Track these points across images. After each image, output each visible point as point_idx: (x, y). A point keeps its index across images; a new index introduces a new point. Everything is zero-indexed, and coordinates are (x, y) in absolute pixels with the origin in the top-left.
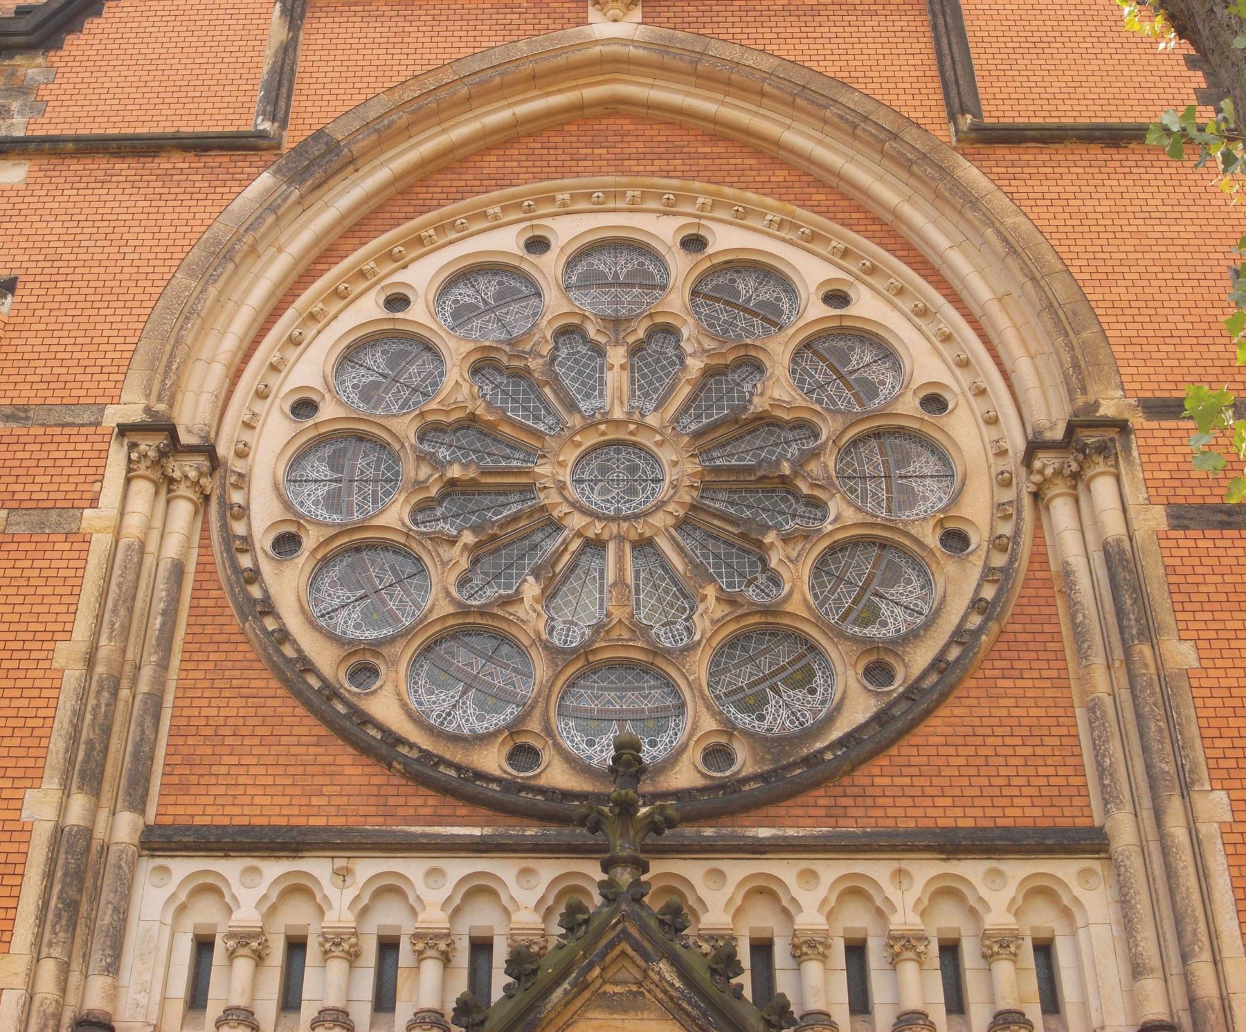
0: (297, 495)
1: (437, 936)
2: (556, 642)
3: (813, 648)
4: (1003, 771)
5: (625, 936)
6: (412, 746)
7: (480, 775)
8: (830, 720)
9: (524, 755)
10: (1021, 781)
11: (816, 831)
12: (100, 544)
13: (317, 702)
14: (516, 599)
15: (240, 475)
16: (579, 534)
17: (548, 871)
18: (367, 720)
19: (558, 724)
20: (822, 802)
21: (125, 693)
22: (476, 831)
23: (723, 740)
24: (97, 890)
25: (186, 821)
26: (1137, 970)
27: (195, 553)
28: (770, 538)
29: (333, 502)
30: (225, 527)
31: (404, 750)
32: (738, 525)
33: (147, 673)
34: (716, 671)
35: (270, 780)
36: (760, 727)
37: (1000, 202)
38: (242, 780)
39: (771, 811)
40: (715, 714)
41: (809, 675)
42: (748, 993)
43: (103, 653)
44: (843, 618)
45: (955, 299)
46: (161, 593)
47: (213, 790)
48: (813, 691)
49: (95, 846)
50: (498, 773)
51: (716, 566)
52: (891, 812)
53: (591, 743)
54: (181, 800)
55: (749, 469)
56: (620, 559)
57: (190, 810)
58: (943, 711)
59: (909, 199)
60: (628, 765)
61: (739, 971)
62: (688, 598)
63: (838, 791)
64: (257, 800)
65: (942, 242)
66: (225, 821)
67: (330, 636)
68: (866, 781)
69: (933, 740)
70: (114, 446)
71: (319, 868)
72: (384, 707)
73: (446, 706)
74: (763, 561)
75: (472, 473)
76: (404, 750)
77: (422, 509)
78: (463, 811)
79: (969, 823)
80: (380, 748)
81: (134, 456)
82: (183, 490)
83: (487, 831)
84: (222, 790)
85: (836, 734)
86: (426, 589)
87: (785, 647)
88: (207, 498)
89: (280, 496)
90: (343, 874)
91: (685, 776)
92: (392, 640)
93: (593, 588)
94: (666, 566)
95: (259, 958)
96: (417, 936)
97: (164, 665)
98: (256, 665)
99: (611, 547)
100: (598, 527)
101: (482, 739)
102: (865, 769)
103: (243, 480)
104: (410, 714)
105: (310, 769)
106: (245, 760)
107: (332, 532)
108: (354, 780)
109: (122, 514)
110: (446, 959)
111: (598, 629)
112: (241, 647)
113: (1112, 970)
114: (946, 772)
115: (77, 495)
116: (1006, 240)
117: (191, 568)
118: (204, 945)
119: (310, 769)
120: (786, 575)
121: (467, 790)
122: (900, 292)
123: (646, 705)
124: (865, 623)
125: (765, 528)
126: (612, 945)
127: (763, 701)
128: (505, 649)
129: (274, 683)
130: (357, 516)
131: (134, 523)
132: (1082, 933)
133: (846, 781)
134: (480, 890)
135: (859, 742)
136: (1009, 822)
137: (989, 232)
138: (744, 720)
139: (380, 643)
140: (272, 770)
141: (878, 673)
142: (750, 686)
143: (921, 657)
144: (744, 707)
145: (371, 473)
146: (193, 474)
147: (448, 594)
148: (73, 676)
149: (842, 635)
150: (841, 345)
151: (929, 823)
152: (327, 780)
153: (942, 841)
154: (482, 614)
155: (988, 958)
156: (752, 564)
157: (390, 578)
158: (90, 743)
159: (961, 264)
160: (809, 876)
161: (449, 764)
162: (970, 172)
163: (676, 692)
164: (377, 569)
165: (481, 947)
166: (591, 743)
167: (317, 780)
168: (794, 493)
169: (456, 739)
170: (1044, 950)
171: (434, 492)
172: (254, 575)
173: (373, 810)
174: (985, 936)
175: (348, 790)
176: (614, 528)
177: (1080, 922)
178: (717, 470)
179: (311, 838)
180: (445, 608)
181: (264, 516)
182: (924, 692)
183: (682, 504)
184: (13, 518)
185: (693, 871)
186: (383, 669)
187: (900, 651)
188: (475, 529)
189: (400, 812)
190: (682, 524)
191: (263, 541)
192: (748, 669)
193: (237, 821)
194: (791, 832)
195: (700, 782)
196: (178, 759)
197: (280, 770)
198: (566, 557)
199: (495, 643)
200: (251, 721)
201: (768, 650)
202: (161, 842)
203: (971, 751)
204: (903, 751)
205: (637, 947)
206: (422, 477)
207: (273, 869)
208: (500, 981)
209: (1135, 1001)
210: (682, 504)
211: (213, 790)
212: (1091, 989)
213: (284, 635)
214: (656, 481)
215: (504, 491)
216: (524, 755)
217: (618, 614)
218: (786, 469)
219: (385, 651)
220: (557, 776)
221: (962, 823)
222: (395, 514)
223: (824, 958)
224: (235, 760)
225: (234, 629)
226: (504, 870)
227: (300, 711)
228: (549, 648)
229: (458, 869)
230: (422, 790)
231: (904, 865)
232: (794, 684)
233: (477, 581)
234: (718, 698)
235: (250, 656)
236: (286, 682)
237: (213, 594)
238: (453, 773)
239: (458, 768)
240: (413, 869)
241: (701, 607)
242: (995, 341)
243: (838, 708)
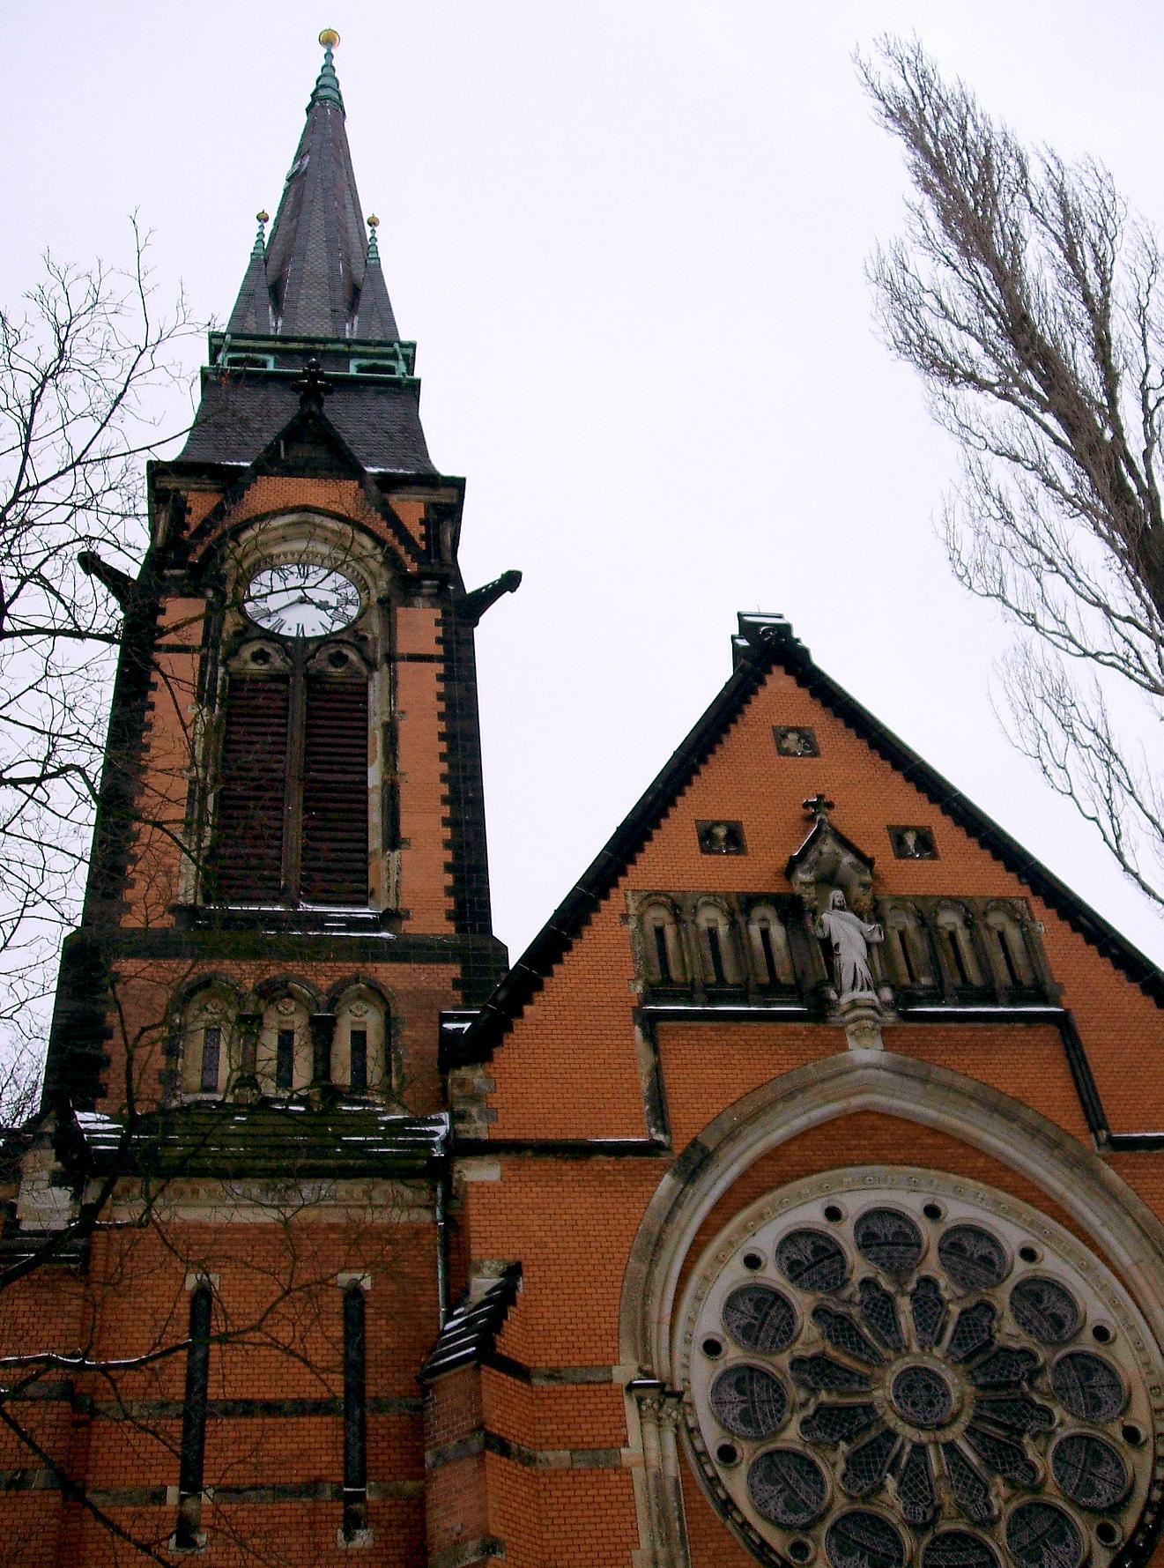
37: (1131, 1196)
45: (1104, 1258)
59: (1069, 1188)
65: (1097, 1223)
70: (626, 1400)
103: (694, 1413)
116: (1139, 1226)
122: (1069, 1253)
131: (653, 1455)
137: (1129, 1221)
150: (1043, 1299)
159: (1108, 1237)
162: (1109, 1173)
181: (712, 1437)
242: (1134, 1290)
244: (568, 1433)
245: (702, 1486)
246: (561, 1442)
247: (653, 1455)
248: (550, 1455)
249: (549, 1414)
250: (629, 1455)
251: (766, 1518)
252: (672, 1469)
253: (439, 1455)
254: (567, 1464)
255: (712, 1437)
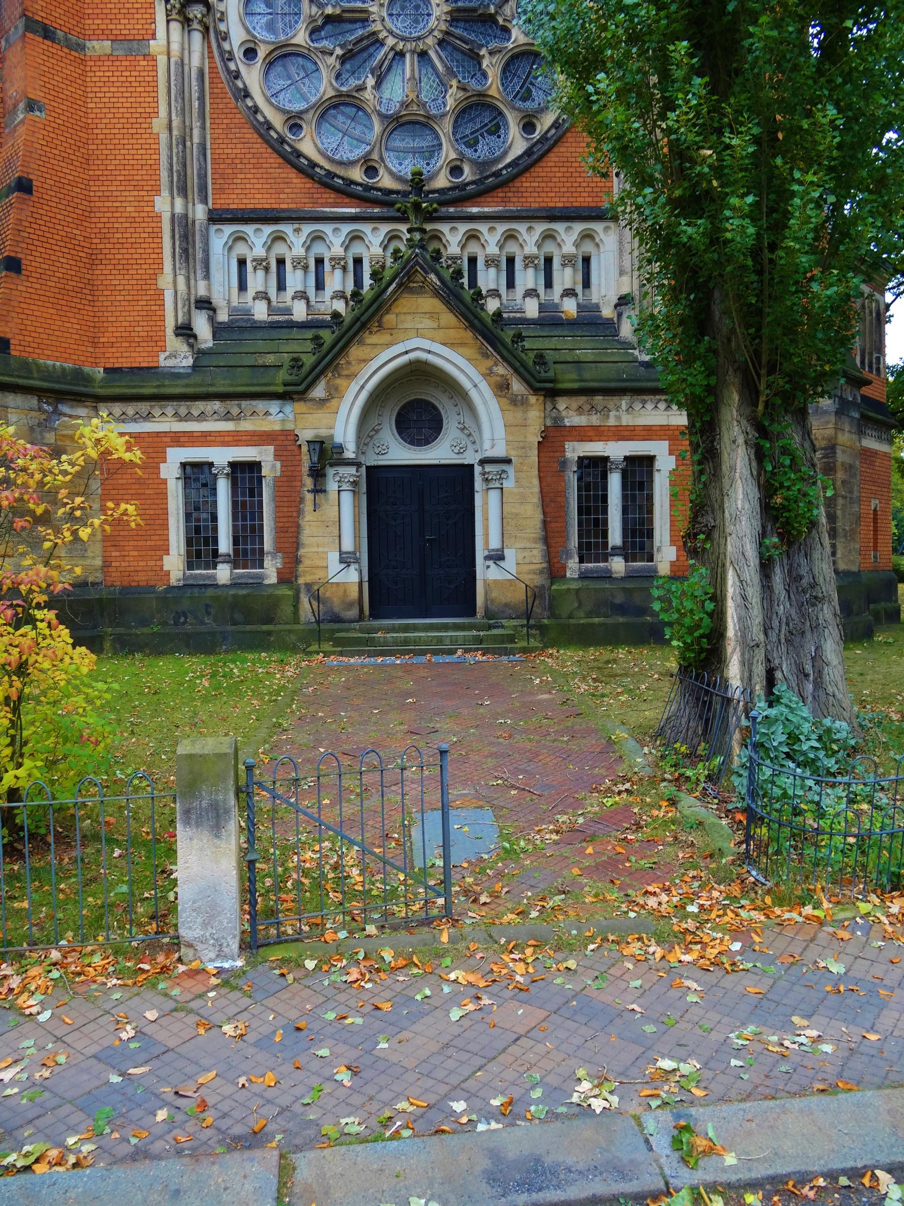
0: (251, 22)
1: (340, 259)
2: (383, 111)
3: (501, 113)
4: (578, 180)
5: (417, 263)
6: (322, 168)
7: (353, 182)
8: (505, 153)
9: (371, 171)
10: (585, 184)
11: (496, 209)
12: (162, 60)
13: (277, 146)
14: (361, 88)
15: (222, 13)
16: (392, 49)
17: (385, 228)
18: (299, 154)
19: (386, 155)
20: (500, 195)
21: (188, 144)
22: (353, 210)
23: (458, 163)
24: (194, 242)
25: (227, 207)
26: (622, 273)
27: (207, 61)
28: (483, 52)
29: (270, 27)
30: (219, 46)
31: (318, 170)
32: (467, 43)
33: (196, 133)
34: (456, 126)
35: (260, 186)
36: (475, 156)
38: (248, 186)
39: (479, 199)
40: (456, 150)
41: (498, 127)
42: (466, 287)
43: (175, 124)
44: (515, 97)
46: (195, 87)
47: (236, 191)
48: (499, 137)
49: (190, 221)
50: (360, 181)
51: (457, 67)
52: (529, 200)
53: (400, 164)
54: (223, 196)
55: (474, 10)
56: (412, 64)
57: (227, 201)
58: (556, 150)
60: (417, 183)
61: (462, 277)
62: (444, 86)
63: (507, 189)
64: (257, 196)
66: (243, 206)
67: (278, 109)
68: (519, 184)
69: (550, 164)
71: (287, 229)
72: (307, 147)
73: (335, 145)
74: (480, 64)
75: (338, 11)
76: (318, 170)
77: (314, 32)
78: (347, 200)
79: (561, 205)
80: (307, 170)
81: (169, 7)
82: (196, 25)
83: (358, 210)
84: (239, 191)
85: (509, 159)
86: (320, 80)
87: (487, 113)
88: (207, 29)
89: (244, 25)
90: (297, 231)
91: (442, 181)
92: (306, 111)
93: (398, 79)
94: (433, 67)
95: (267, 269)
96: (331, 259)
97: (203, 128)
98: (246, 126)
99: (408, 56)
100: (401, 44)
101: (352, 163)
102: (519, 179)
104: (319, 151)
105: (278, 181)
106: (248, 176)
107: (272, 47)
108: (298, 186)
109: (168, 42)
110: (344, 269)
111: (402, 104)
112: (238, 116)
113: (614, 271)
114: (554, 180)
115: (144, 32)
117: (207, 70)
118: (242, 263)
119: (278, 181)
120: (490, 73)
121: (346, 191)
123: (424, 144)
124: (524, 100)
125: (481, 46)
126: (412, 267)
127: (477, 142)
128: (360, 113)
129: (256, 136)
130: (282, 38)
131: (175, 47)
132: (602, 255)
133: (511, 185)
134: (356, 237)
135: (518, 165)
136: (578, 204)
138: (468, 152)
139: (302, 112)
140: (261, 181)
141: (528, 127)
142: (472, 133)
143: (547, 121)
144: (468, 145)
145: (286, 10)
146: (199, 16)
147: (331, 84)
148: (164, 137)
149: (514, 108)
151: (544, 205)
152: (285, 186)
153: (549, 214)
154: (348, 96)
155: (564, 265)
156: (474, 66)
157: (302, 74)
158: (178, 171)
160: (492, 229)
161: (339, 177)
163: (437, 137)
164: (293, 67)
165: (358, 261)
166: (400, 164)
167: (282, 186)
168: (496, 22)
169: (341, 163)
170: (587, 260)
171: (320, 22)
172: (237, 75)
173: (307, 200)
174: (563, 257)
175: (296, 191)
176: (409, 46)
177: (602, 249)
178: (458, 10)
179: (283, 215)
180: (331, 93)
181: (237, 37)
182: (547, 139)
183: (441, 31)
184: (115, 46)
185: (445, 228)
186: (304, 126)
187: (539, 116)
188: (342, 46)
189: (320, 201)
190: (441, 43)
191: (238, 54)
192: (470, 125)
193: (249, 206)
194: (486, 209)
195: (448, 185)
196: (217, 176)
197: (264, 181)
198: (386, 62)
199: (354, 110)
200: (248, 156)
201: (480, 114)
202: (217, 217)
203: (565, 169)
204: (537, 170)
205: (422, 268)
206: (313, 13)
207: (268, 229)
208: (367, 281)
209: (619, 287)
210: (441, 31)
211: (236, 191)
212: (603, 280)
213: (256, 110)
214: (429, 15)
215: (353, 21)
216: (371, 171)
217: (412, 96)
218: (492, 9)
219: (304, 116)
220: (386, 181)
221: (559, 205)
222: (301, 38)
223: (497, 266)
224: (243, 176)
225: (232, 106)
226: (366, 228)
227: (270, 150)
228: (379, 114)
229: (346, 228)
230: (328, 190)
231: (533, 225)
232: (490, 133)
233: (345, 76)
234: (457, 140)
235: (243, 121)
236: (261, 136)
237: (220, 85)
238: (340, 181)
239: (343, 178)
240: (327, 228)
241: (450, 91)
243: (510, 147)
244: (110, 27)
245: (223, 75)
246: (103, 35)
247: (175, 47)
248: (95, 43)
249: (96, 11)
250: (156, 46)
251: (271, 104)
252: (196, 61)
253: (7, 41)
254: (109, 52)
255: (237, 37)
